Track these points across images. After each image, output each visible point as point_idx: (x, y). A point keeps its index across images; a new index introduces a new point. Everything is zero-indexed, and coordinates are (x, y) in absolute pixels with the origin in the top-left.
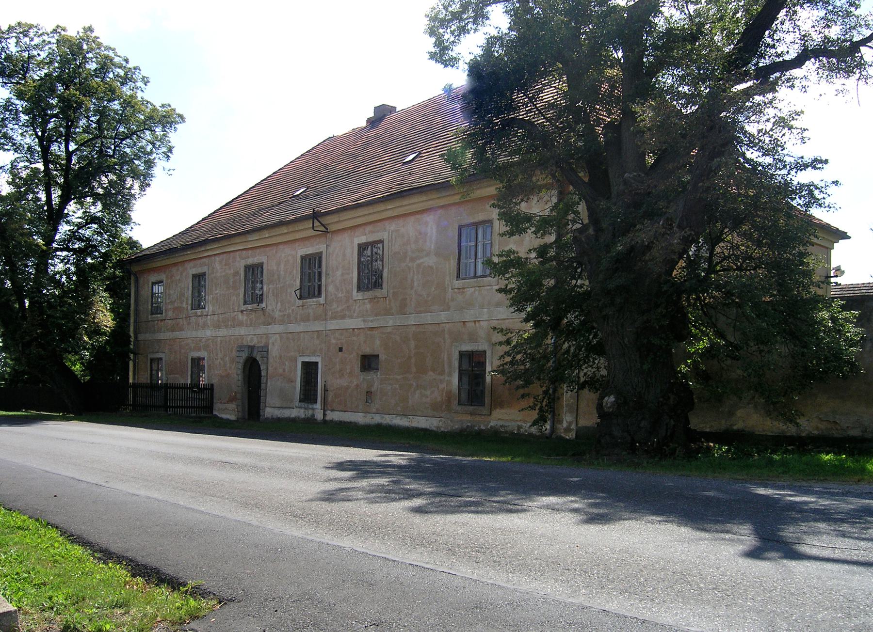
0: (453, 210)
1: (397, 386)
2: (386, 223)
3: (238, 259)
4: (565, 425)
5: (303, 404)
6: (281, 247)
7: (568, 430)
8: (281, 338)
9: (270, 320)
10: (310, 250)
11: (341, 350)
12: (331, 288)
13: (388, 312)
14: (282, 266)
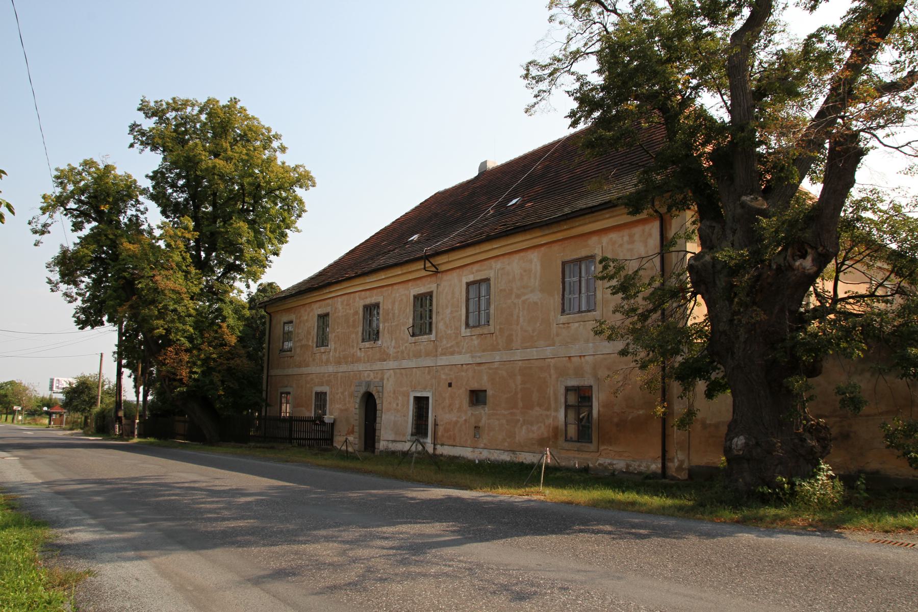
0: (556, 247)
1: (504, 422)
2: (492, 262)
3: (357, 299)
4: (676, 463)
5: (414, 438)
6: (395, 287)
7: (680, 469)
8: (395, 374)
9: (384, 357)
10: (421, 289)
11: (450, 385)
12: (441, 326)
13: (494, 348)
14: (397, 304)
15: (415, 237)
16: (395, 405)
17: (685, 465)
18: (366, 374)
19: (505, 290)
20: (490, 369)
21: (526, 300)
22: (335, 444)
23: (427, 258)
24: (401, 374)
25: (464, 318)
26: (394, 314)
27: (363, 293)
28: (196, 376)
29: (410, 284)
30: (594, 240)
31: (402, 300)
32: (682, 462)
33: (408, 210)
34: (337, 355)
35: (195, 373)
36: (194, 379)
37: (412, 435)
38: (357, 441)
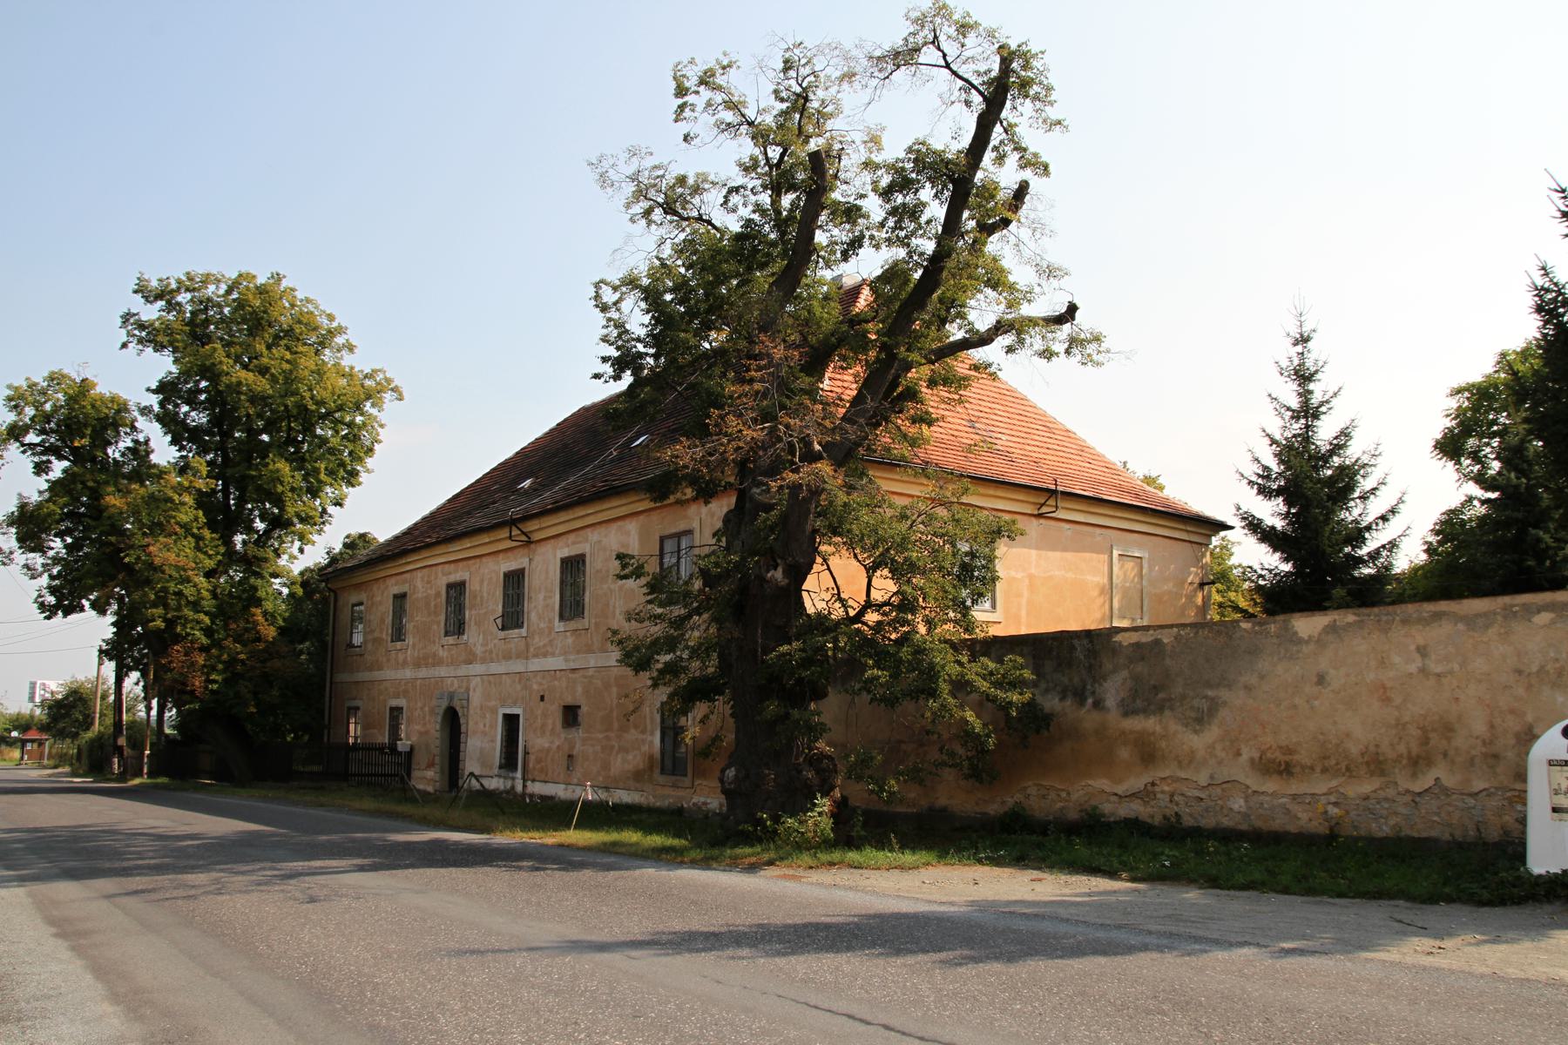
11: (542, 698)
12: (533, 616)
13: (589, 650)
15: (527, 483)
23: (513, 523)
28: (215, 686)
29: (501, 556)
33: (539, 434)
35: (214, 681)
36: (212, 691)
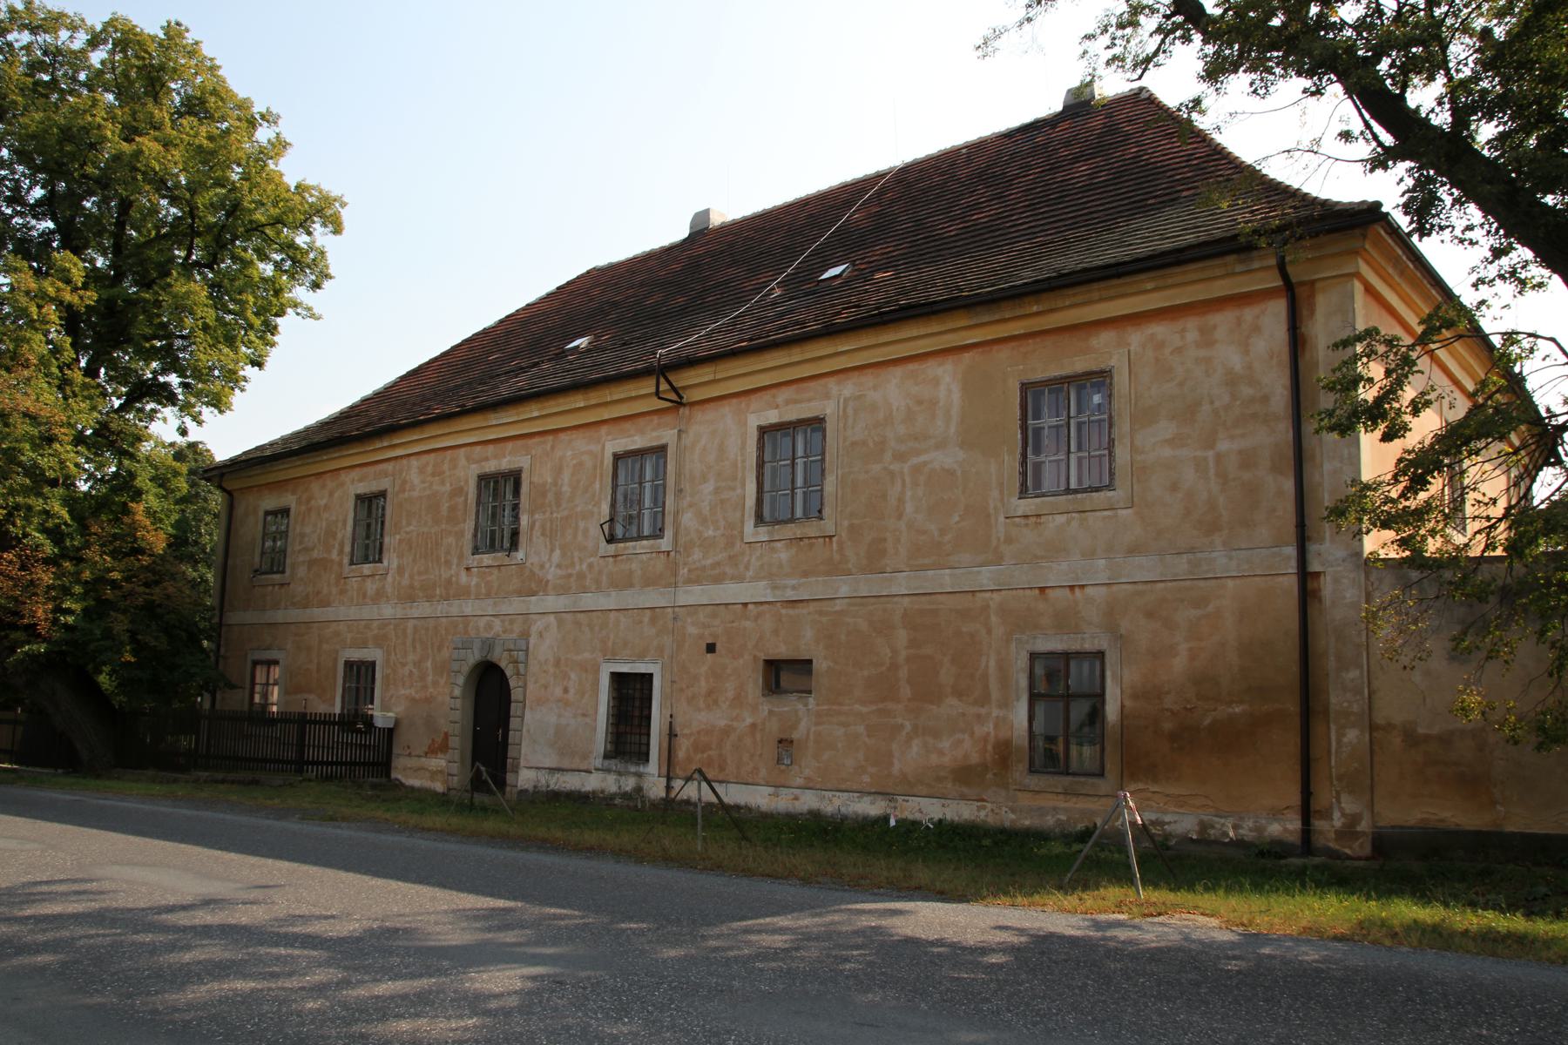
0: (1003, 354)
1: (861, 729)
2: (831, 383)
3: (463, 462)
4: (1338, 821)
5: (613, 764)
6: (562, 436)
7: (1348, 833)
8: (560, 623)
9: (533, 585)
10: (637, 440)
11: (711, 648)
12: (687, 519)
13: (835, 569)
14: (566, 476)
15: (582, 342)
16: (558, 692)
17: (1364, 826)
18: (482, 622)
19: (864, 443)
20: (821, 613)
21: (925, 463)
22: (393, 775)
23: (662, 371)
24: (578, 624)
25: (751, 502)
26: (558, 495)
27: (478, 448)
28: (70, 619)
29: (604, 429)
30: (1105, 338)
31: (581, 464)
32: (1354, 819)
33: (531, 299)
34: (406, 582)
35: (69, 612)
36: (66, 626)
37: (606, 756)
38: (455, 768)
